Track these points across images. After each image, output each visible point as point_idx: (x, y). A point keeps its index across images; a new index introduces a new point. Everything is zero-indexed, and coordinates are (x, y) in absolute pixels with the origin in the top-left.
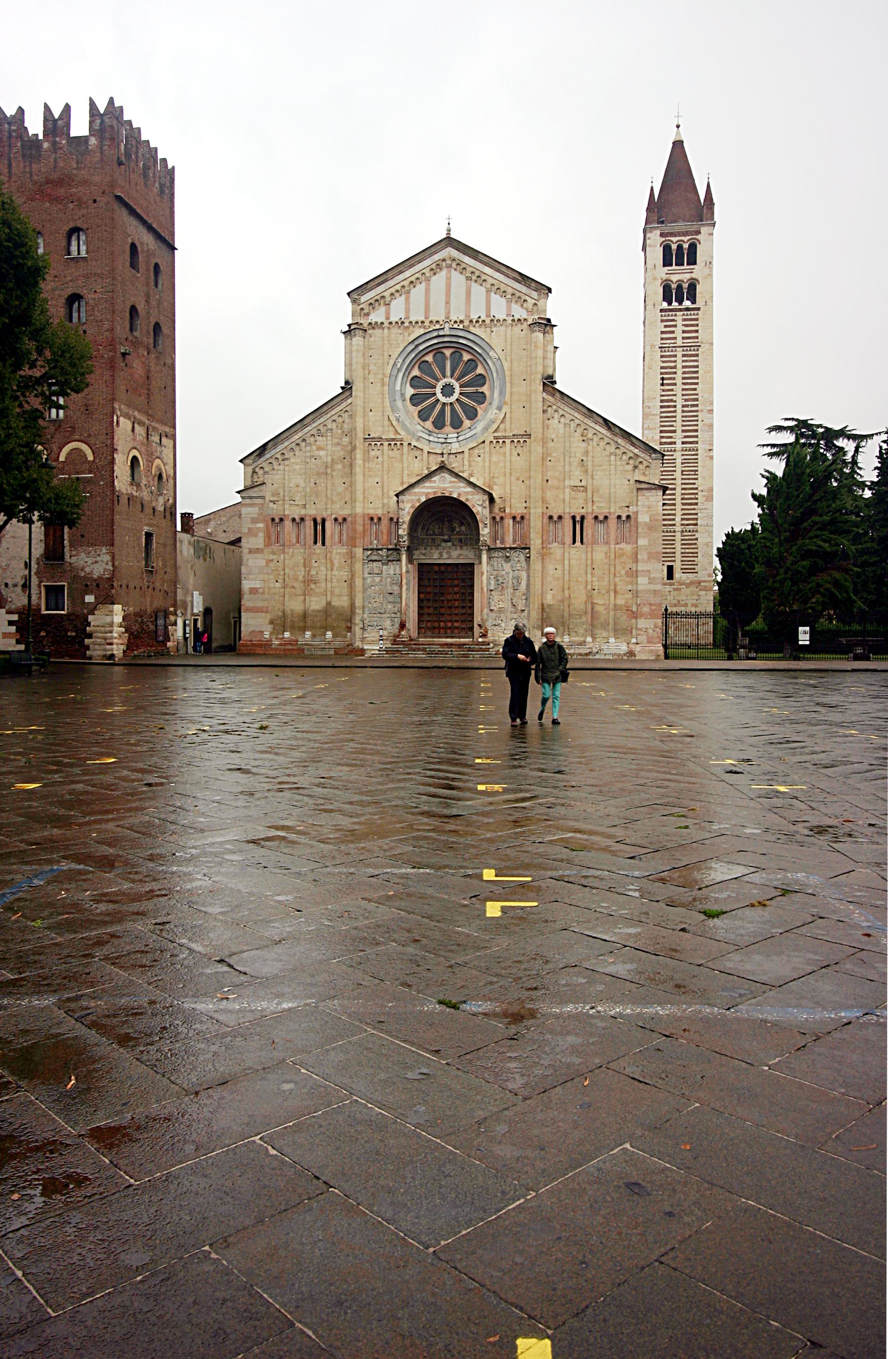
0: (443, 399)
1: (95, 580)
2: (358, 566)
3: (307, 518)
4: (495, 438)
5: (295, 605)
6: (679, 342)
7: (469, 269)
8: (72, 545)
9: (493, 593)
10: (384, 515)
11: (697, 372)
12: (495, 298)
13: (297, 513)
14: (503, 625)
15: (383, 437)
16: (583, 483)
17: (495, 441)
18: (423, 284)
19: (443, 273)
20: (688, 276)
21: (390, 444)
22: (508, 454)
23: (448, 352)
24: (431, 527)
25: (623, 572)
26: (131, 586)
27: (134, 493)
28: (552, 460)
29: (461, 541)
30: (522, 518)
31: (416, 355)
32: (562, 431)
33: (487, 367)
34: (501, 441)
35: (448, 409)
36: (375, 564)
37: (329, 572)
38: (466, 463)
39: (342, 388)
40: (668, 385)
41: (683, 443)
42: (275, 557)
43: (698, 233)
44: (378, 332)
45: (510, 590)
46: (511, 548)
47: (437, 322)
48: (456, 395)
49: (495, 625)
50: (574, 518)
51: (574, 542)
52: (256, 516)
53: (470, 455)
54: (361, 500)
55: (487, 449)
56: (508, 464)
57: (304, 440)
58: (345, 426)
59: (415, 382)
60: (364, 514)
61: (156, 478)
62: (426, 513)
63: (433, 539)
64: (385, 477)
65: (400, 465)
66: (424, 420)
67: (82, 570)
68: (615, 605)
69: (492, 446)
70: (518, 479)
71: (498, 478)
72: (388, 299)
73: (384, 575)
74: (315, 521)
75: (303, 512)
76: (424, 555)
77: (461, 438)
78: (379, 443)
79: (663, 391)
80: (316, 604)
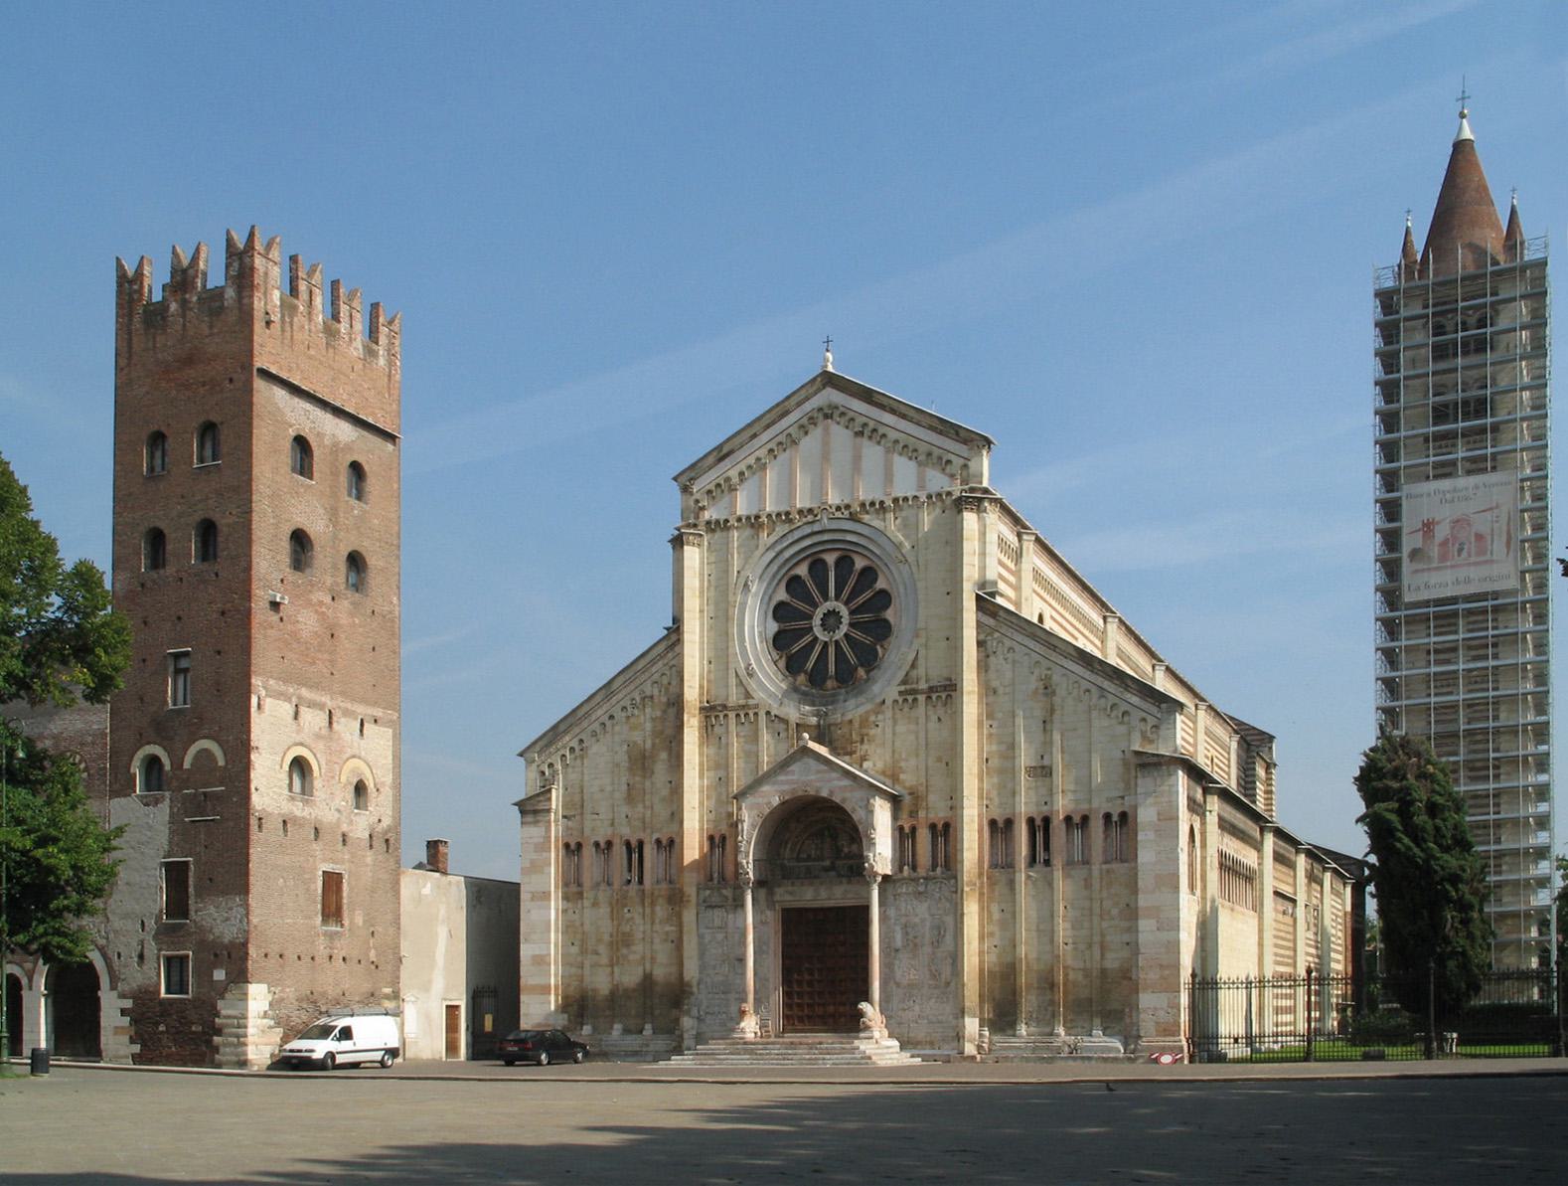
0: (822, 636)
1: (226, 947)
2: (689, 916)
3: (617, 842)
4: (901, 693)
5: (601, 983)
8: (198, 895)
9: (900, 955)
12: (904, 468)
14: (917, 1008)
16: (1046, 762)
19: (816, 433)
22: (922, 720)
23: (830, 559)
25: (1115, 912)
26: (291, 956)
27: (298, 813)
30: (947, 826)
31: (780, 568)
32: (1009, 675)
33: (891, 579)
35: (831, 650)
36: (717, 912)
37: (648, 926)
39: (667, 629)
42: (570, 905)
45: (927, 949)
47: (810, 511)
48: (844, 628)
49: (905, 1010)
50: (1031, 821)
52: (542, 840)
55: (889, 714)
56: (922, 735)
58: (672, 689)
59: (780, 612)
61: (352, 788)
63: (808, 869)
67: (210, 931)
68: (1103, 972)
70: (939, 759)
72: (735, 480)
73: (730, 930)
74: (628, 844)
75: (609, 831)
76: (791, 893)
80: (630, 977)
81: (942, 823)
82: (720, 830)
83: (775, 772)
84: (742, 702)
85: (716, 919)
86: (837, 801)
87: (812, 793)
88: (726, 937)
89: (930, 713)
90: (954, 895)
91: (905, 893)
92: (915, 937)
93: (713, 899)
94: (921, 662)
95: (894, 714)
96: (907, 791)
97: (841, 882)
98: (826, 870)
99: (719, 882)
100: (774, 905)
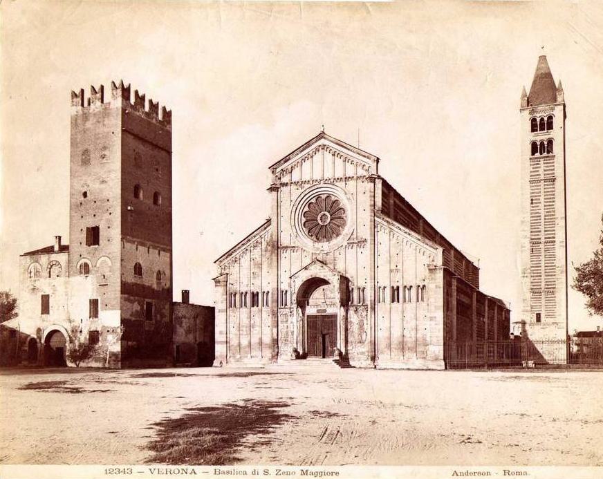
4: (348, 243)
6: (542, 177)
7: (334, 150)
11: (554, 195)
13: (244, 289)
18: (310, 159)
20: (548, 137)
30: (364, 288)
40: (536, 203)
41: (546, 238)
43: (553, 109)
44: (284, 189)
48: (328, 220)
51: (393, 301)
57: (247, 250)
74: (253, 293)
79: (533, 207)
94: (355, 233)
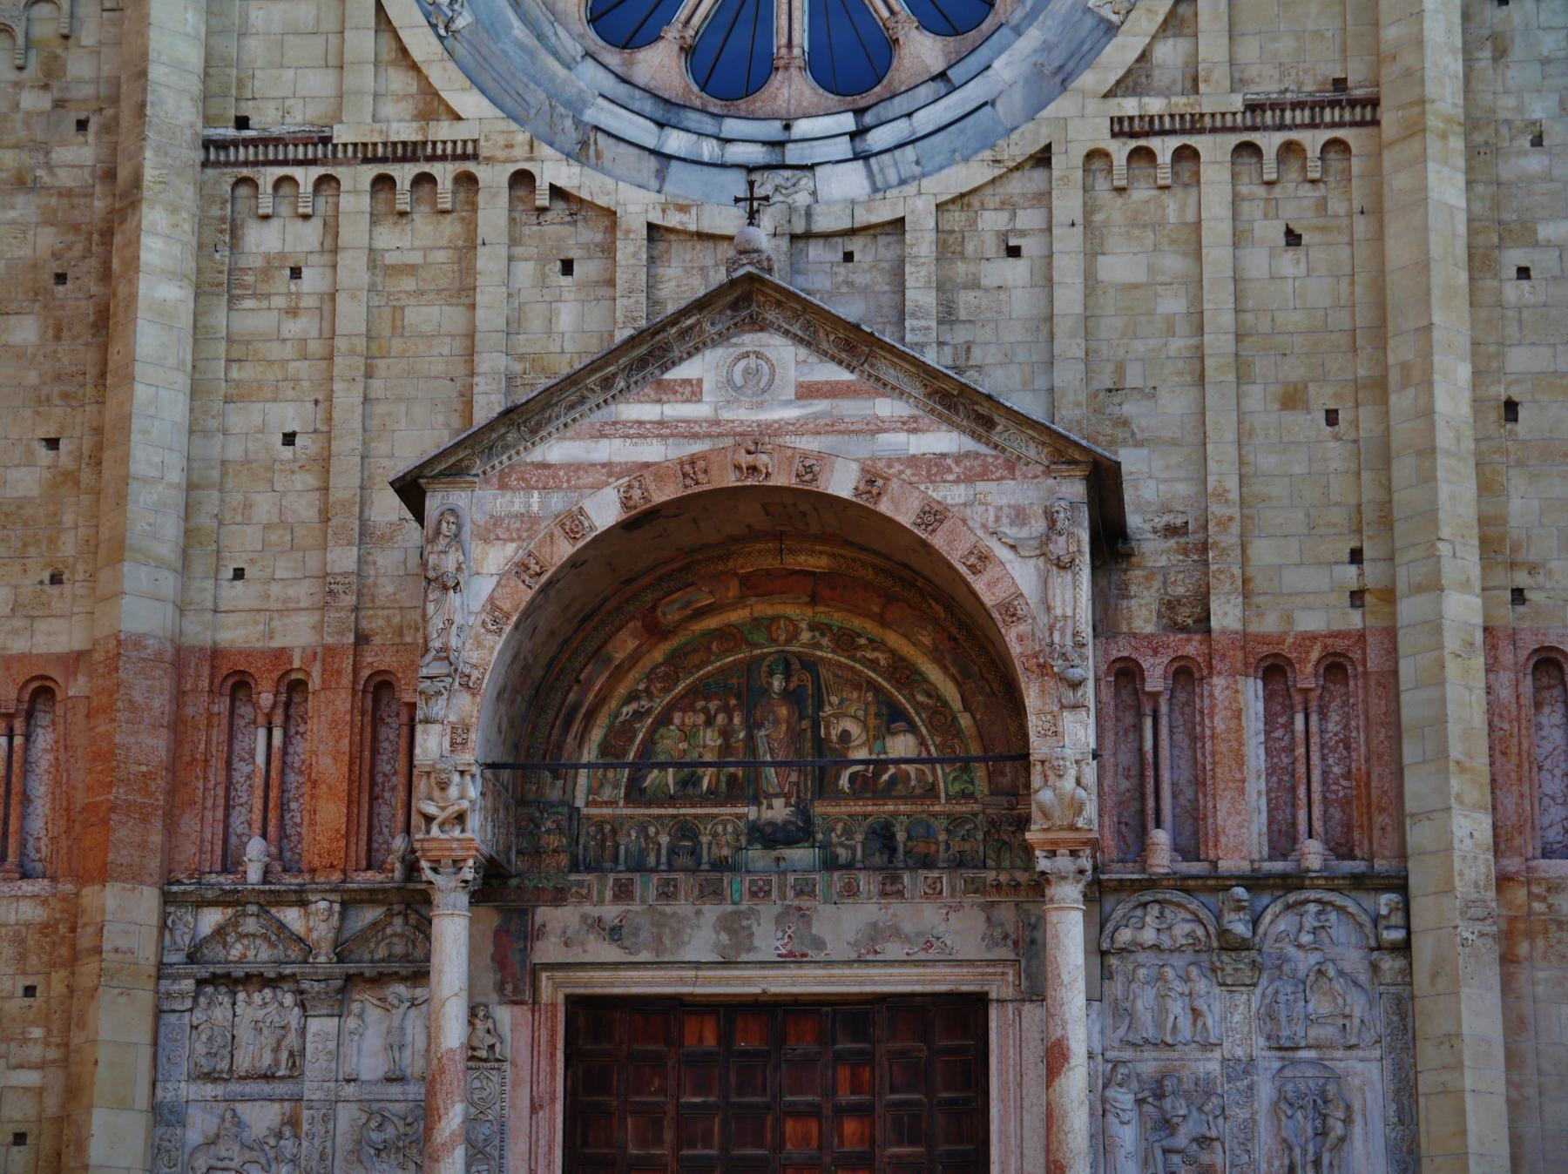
4: (1121, 128)
10: (330, 651)
15: (342, 134)
17: (1120, 151)
21: (384, 183)
24: (670, 743)
28: (1543, 263)
29: (883, 835)
34: (1164, 148)
36: (252, 1008)
38: (920, 296)
46: (1255, 882)
53: (948, 247)
54: (167, 550)
55: (1068, 204)
58: (79, 67)
60: (180, 658)
62: (625, 644)
64: (347, 398)
65: (451, 317)
66: (632, 38)
69: (1101, 185)
70: (1292, 399)
71: (1151, 394)
76: (615, 933)
77: (878, 139)
78: (306, 177)
81: (1315, 655)
82: (281, 654)
83: (607, 383)
84: (406, 132)
85: (245, 1033)
86: (906, 519)
87: (782, 479)
88: (293, 1122)
89: (1249, 210)
90: (1390, 964)
91: (1156, 947)
92: (1204, 1141)
93: (235, 953)
95: (1089, 210)
96: (1160, 522)
97: (851, 891)
98: (769, 837)
99: (267, 871)
100: (535, 988)
